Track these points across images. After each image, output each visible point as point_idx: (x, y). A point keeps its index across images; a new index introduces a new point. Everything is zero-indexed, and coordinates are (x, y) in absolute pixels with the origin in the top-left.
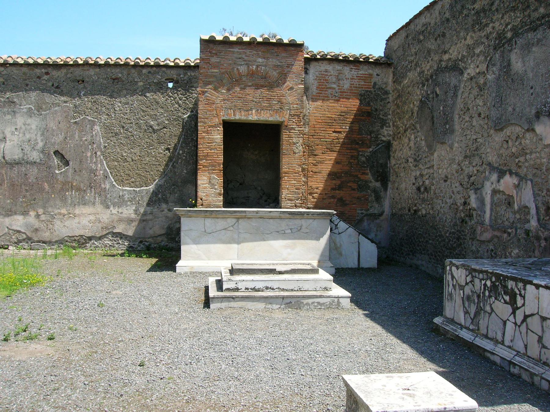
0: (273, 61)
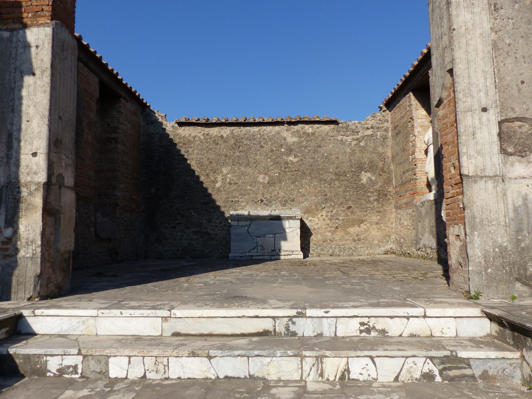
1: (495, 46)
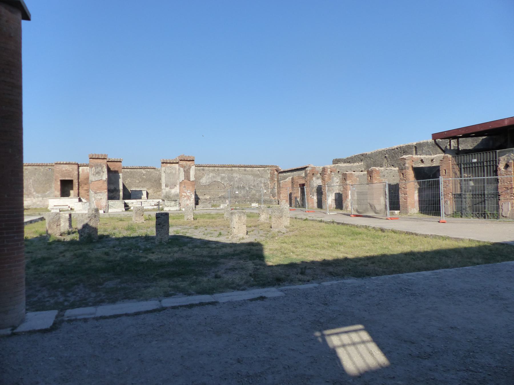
0: (71, 167)
1: (165, 177)
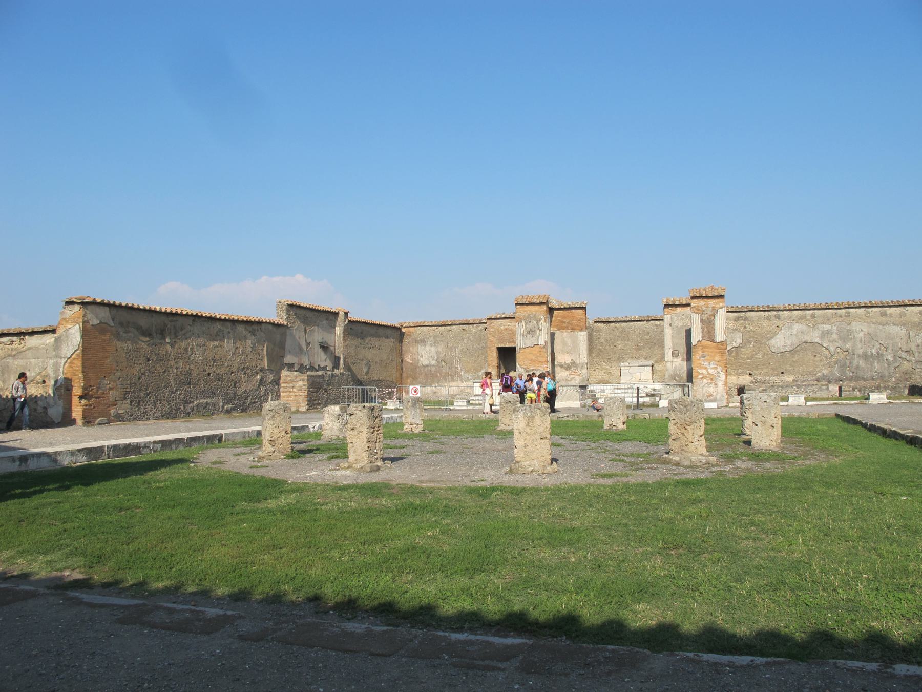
1: (672, 336)
